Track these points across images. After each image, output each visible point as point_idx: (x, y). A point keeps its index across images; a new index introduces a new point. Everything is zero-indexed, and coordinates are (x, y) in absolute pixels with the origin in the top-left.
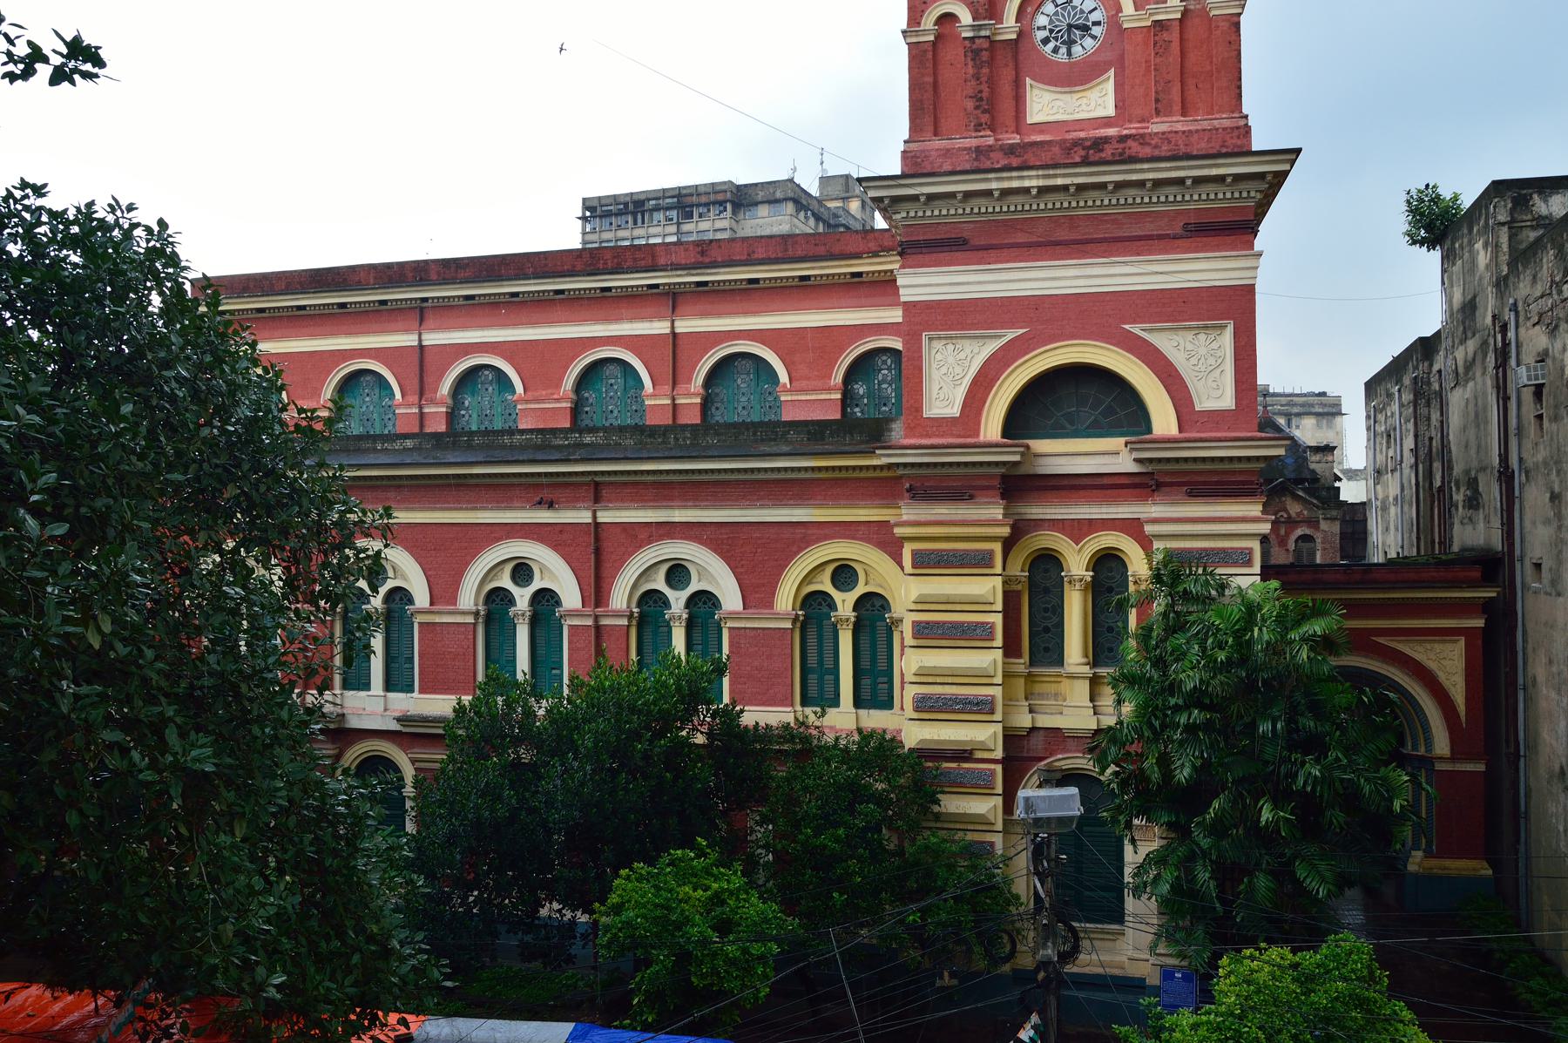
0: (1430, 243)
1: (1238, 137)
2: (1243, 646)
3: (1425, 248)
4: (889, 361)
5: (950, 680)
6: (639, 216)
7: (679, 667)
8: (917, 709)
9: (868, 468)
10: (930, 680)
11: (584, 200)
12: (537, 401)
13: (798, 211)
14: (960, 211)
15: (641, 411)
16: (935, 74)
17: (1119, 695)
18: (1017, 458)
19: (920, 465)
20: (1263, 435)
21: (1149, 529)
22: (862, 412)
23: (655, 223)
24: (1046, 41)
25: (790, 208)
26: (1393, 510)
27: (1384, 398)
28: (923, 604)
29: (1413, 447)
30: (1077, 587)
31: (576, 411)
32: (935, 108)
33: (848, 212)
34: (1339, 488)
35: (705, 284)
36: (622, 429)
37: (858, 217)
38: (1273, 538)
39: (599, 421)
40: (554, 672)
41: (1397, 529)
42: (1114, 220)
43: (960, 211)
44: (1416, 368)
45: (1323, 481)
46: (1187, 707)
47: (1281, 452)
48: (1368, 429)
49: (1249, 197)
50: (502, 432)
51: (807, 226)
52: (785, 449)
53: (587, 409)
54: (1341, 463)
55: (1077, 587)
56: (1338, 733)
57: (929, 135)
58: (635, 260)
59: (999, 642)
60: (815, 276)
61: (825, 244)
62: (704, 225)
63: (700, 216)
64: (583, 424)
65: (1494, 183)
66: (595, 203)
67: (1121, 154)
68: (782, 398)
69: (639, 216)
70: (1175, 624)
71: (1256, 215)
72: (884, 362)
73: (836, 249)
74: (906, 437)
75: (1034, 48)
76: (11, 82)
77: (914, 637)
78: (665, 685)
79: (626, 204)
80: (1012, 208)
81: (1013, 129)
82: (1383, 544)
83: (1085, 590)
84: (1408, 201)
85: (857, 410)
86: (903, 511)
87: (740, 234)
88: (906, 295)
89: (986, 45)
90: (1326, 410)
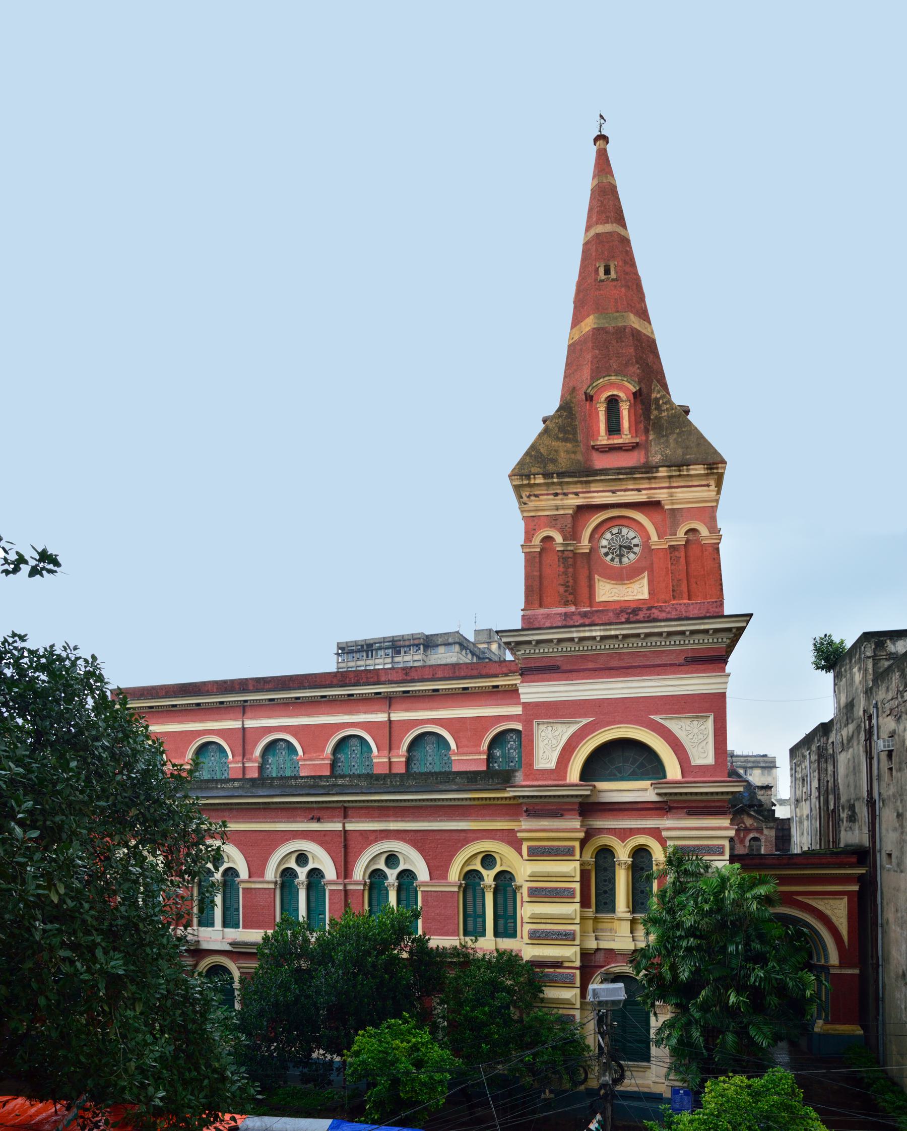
0: (827, 668)
1: (716, 607)
2: (719, 901)
3: (824, 671)
4: (514, 737)
5: (549, 921)
6: (370, 653)
7: (393, 914)
8: (530, 938)
9: (502, 798)
10: (538, 921)
11: (338, 643)
12: (311, 759)
13: (462, 650)
14: (555, 650)
15: (371, 765)
16: (540, 571)
17: (647, 929)
18: (588, 793)
19: (532, 797)
20: (731, 779)
21: (664, 834)
22: (499, 766)
23: (379, 657)
24: (606, 554)
25: (457, 648)
26: (806, 823)
27: (801, 758)
28: (534, 877)
29: (817, 786)
30: (623, 867)
31: (333, 766)
32: (540, 590)
33: (491, 650)
34: (774, 810)
35: (408, 692)
36: (359, 776)
37: (497, 653)
38: (736, 839)
39: (346, 771)
40: (320, 916)
41: (808, 834)
42: (644, 655)
43: (555, 650)
44: (819, 741)
45: (765, 806)
46: (687, 937)
47: (741, 789)
48: (791, 776)
49: (722, 642)
50: (290, 778)
51: (466, 658)
52: (454, 787)
53: (340, 764)
54: (776, 795)
55: (623, 867)
56: (774, 952)
57: (537, 606)
58: (367, 678)
59: (578, 899)
60: (472, 688)
61: (477, 669)
62: (407, 658)
63: (405, 652)
64: (337, 773)
65: (864, 633)
66: (344, 645)
67: (648, 617)
68: (453, 758)
69: (370, 653)
70: (680, 889)
71: (727, 652)
72: (512, 737)
73: (484, 672)
74: (524, 780)
75: (600, 557)
76: (7, 575)
77: (529, 896)
78: (385, 924)
79: (362, 646)
80: (586, 648)
81: (588, 604)
82: (800, 843)
83: (628, 869)
84: (815, 645)
85: (496, 765)
86: (523, 823)
87: (429, 663)
88: (524, 698)
89: (571, 555)
90: (767, 765)
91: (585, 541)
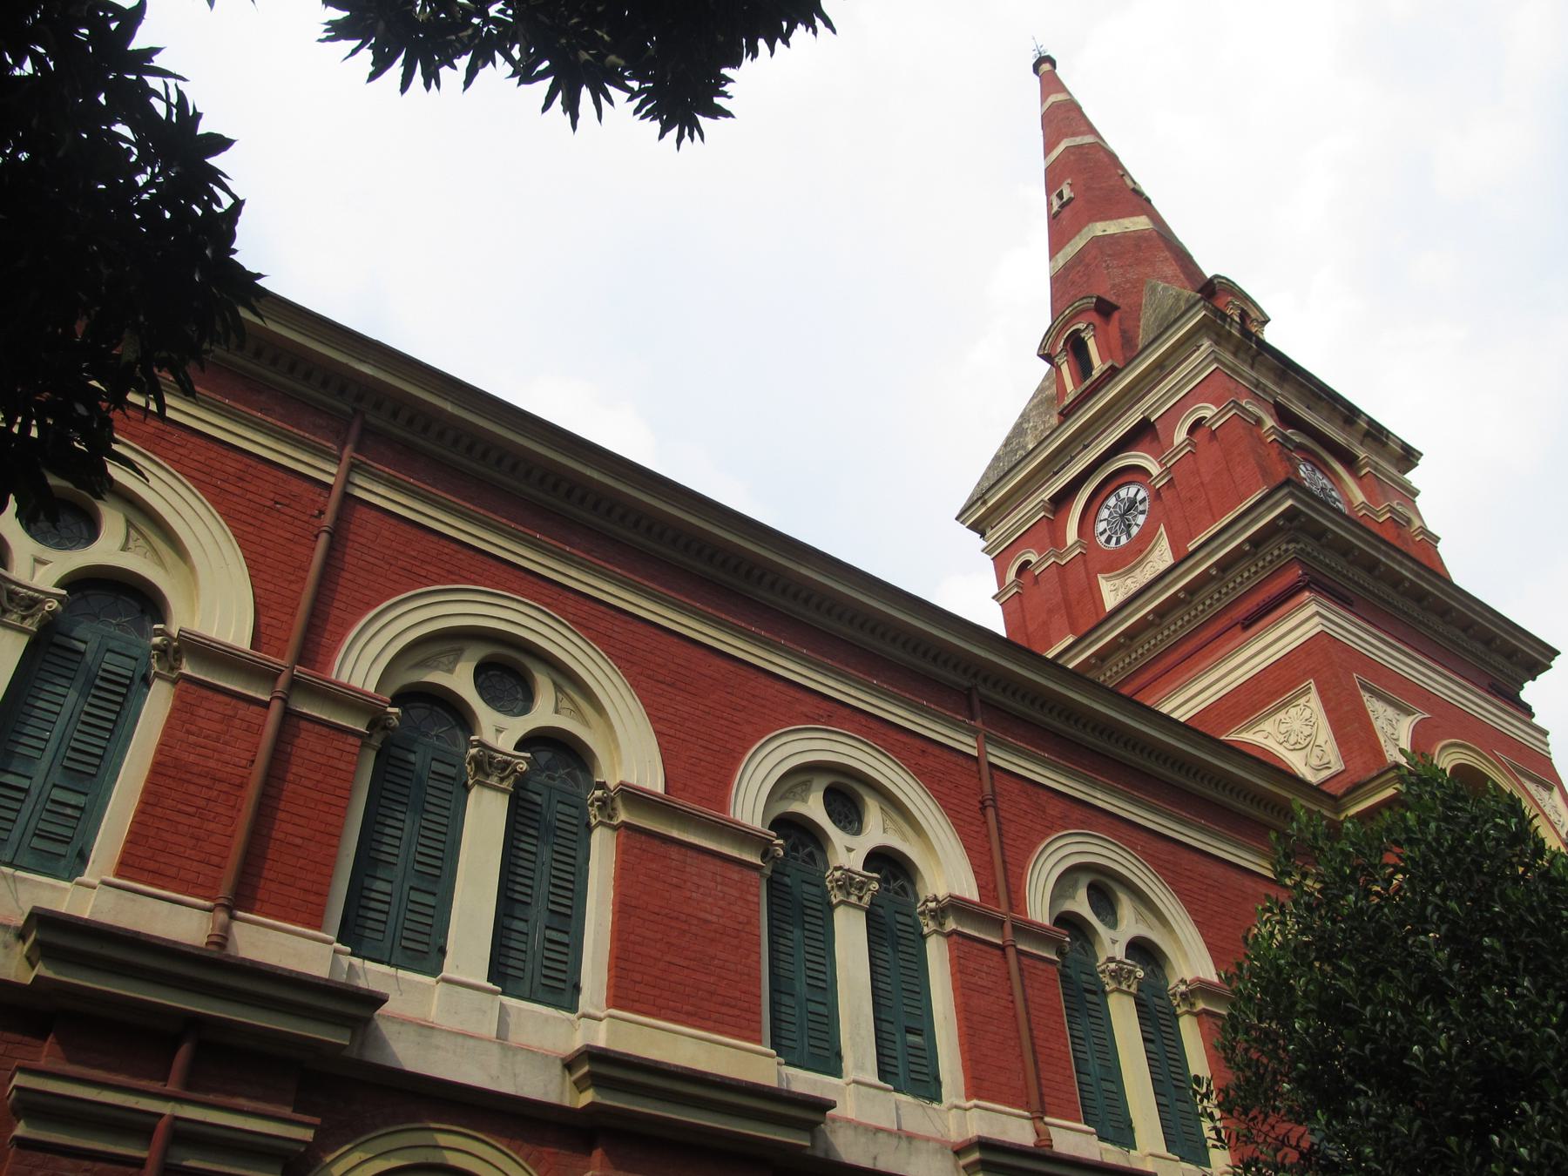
24: (1108, 540)
91: (1072, 534)
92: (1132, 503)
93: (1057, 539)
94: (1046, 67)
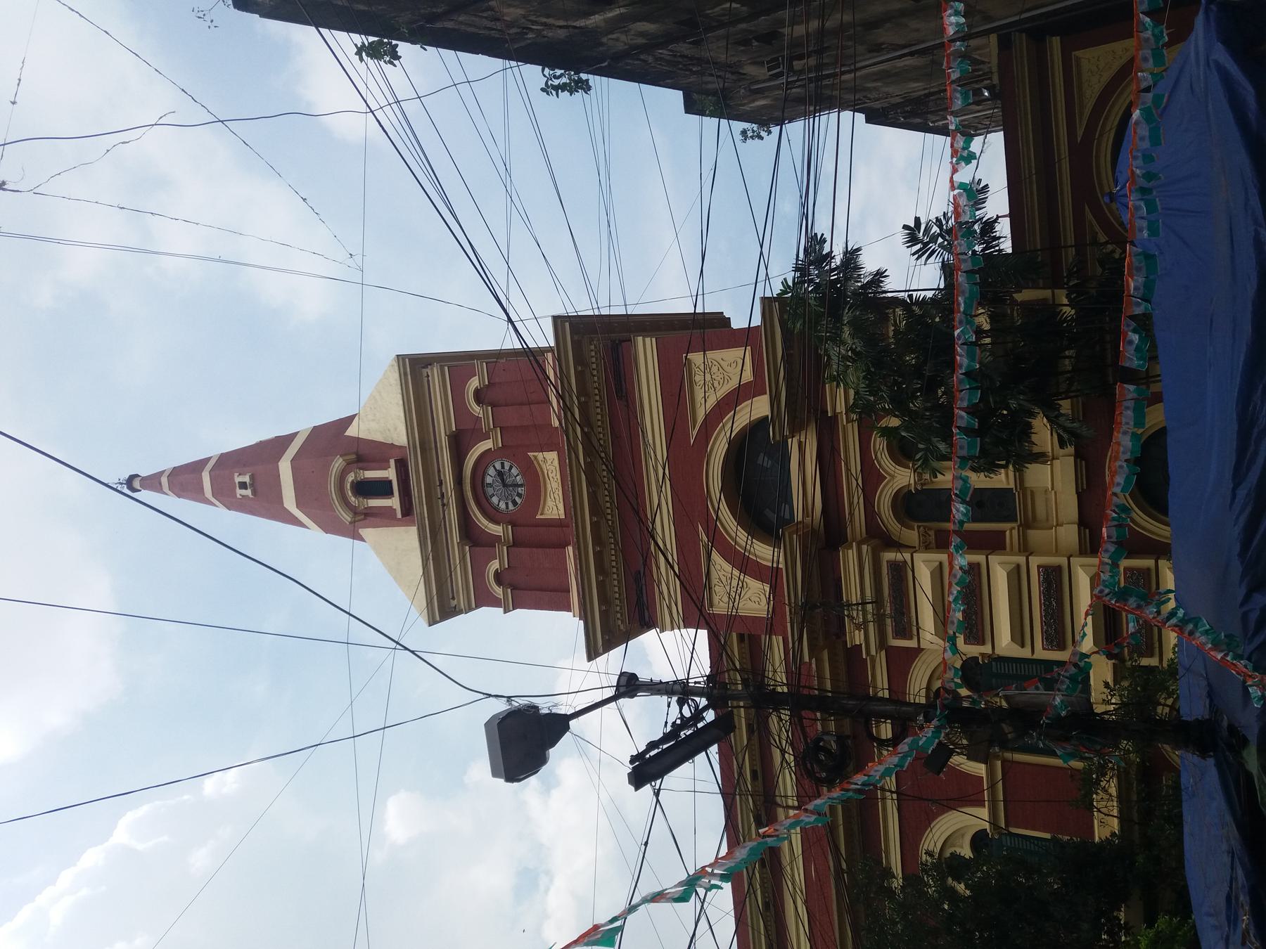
24: (515, 503)
77: (983, 643)
91: (496, 530)
92: (500, 474)
93: (492, 541)
94: (136, 484)
